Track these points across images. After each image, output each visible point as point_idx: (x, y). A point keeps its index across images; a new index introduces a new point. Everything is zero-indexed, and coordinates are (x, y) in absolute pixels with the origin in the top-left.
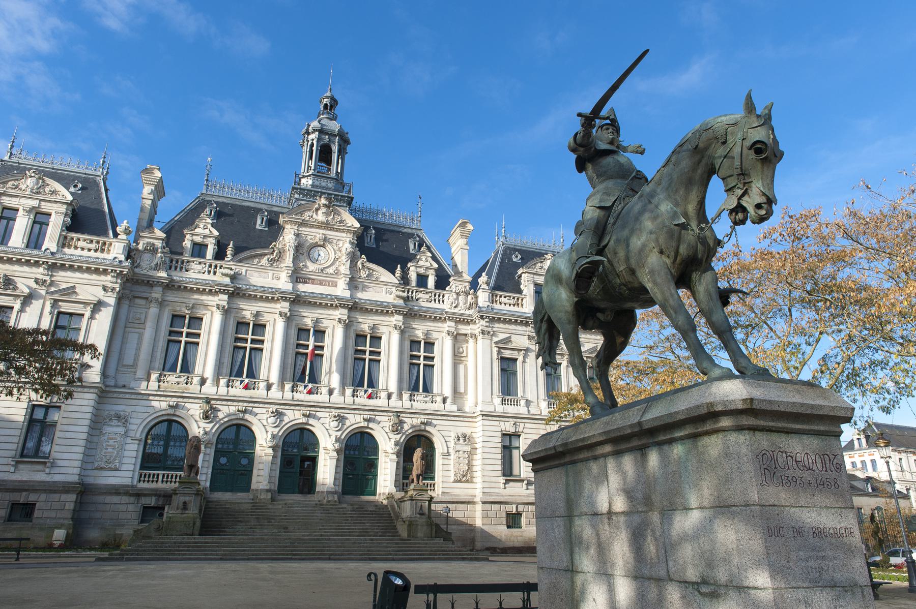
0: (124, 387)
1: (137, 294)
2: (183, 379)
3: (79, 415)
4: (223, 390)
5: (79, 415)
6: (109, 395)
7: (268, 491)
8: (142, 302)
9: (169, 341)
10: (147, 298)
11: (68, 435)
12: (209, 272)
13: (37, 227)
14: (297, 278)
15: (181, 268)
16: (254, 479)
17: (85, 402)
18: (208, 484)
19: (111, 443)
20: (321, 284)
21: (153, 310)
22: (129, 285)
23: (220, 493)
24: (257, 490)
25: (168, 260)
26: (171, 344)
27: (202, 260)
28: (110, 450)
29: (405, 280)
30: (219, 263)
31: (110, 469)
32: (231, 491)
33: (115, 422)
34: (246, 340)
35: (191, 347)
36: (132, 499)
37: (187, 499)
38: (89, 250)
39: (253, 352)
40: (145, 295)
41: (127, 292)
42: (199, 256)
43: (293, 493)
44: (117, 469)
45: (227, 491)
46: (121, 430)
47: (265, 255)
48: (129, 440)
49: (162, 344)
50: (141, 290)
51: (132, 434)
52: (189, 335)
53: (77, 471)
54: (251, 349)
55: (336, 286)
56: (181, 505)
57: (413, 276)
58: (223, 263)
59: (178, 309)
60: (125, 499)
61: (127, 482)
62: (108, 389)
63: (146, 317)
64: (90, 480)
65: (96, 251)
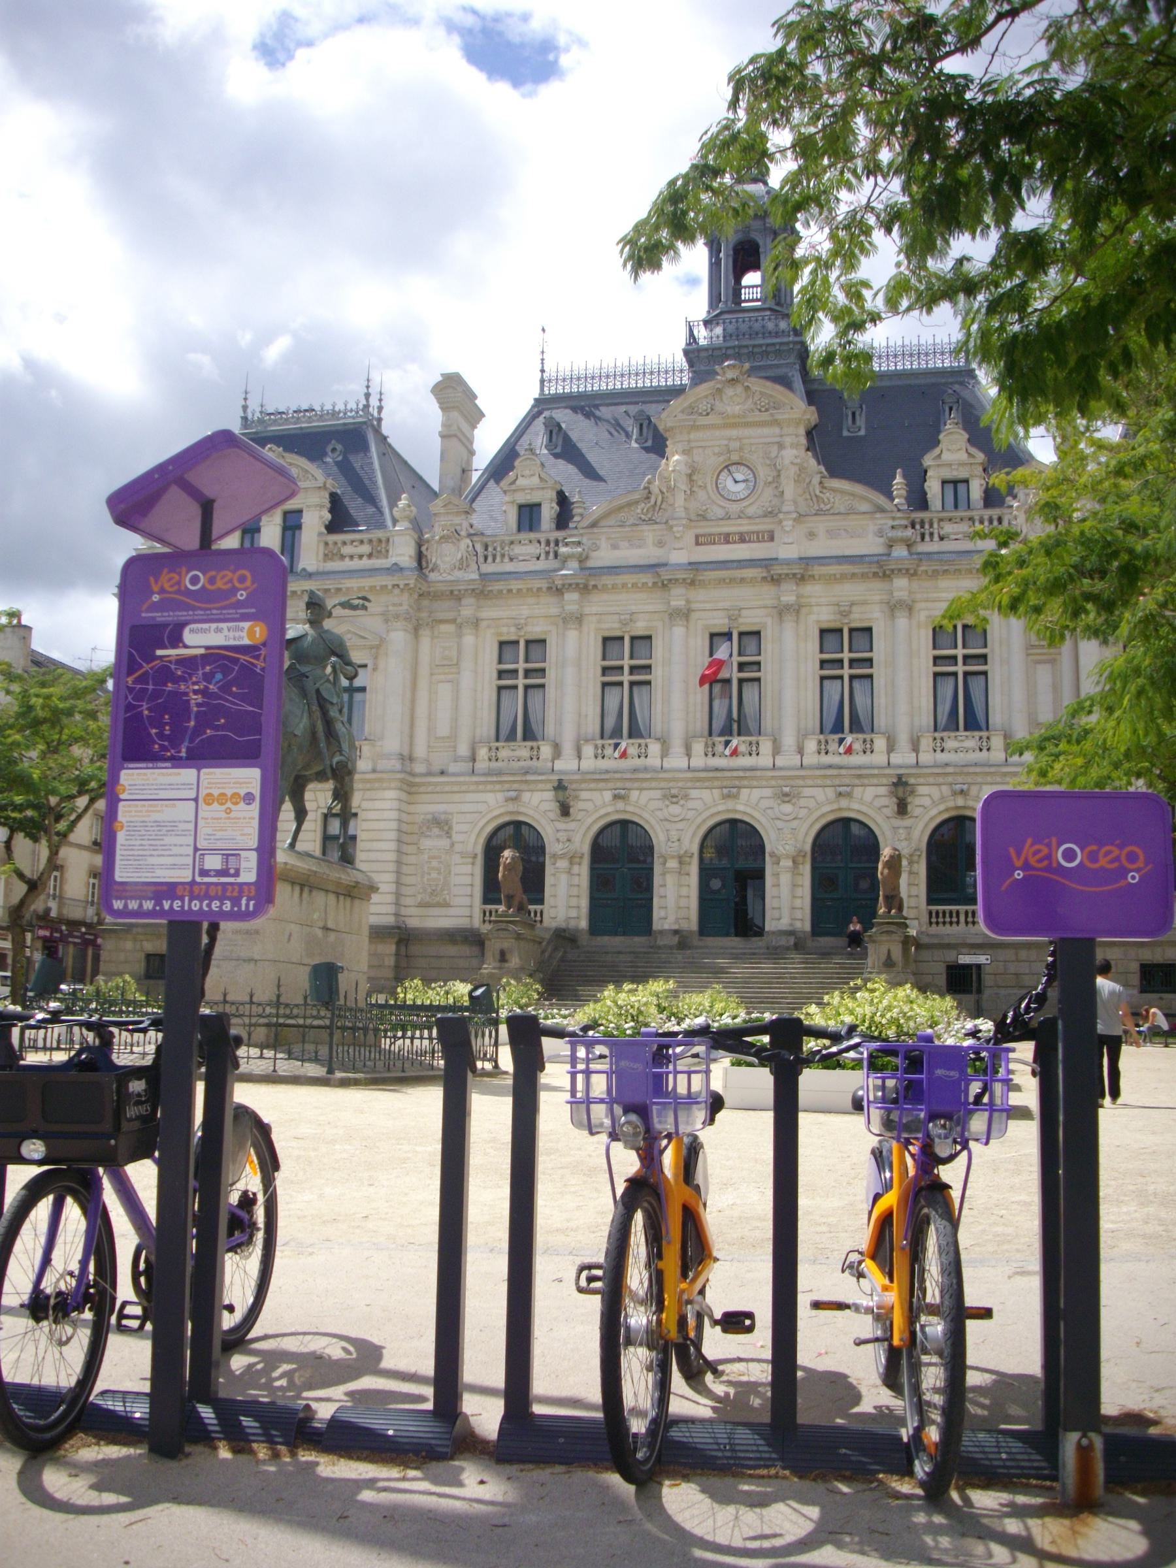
0: (442, 773)
1: (441, 616)
2: (525, 753)
3: (382, 825)
4: (588, 763)
5: (382, 825)
6: (422, 789)
7: (676, 932)
8: (450, 628)
9: (500, 688)
10: (453, 621)
11: (372, 856)
12: (547, 553)
13: (289, 533)
14: (697, 537)
15: (503, 556)
16: (657, 914)
17: (387, 805)
18: (584, 924)
19: (435, 863)
20: (742, 540)
21: (469, 640)
22: (425, 603)
23: (606, 938)
24: (661, 932)
25: (479, 547)
26: (504, 693)
27: (532, 535)
28: (434, 875)
29: (919, 500)
30: (560, 535)
31: (438, 905)
32: (624, 934)
33: (436, 831)
34: (621, 668)
35: (535, 695)
36: (475, 950)
37: (506, 945)
38: (361, 557)
39: (635, 689)
40: (450, 615)
41: (424, 615)
42: (531, 530)
43: (727, 935)
44: (447, 905)
45: (616, 934)
46: (444, 843)
47: (637, 502)
48: (456, 858)
49: (489, 695)
50: (443, 609)
51: (458, 848)
52: (528, 673)
53: (391, 909)
54: (632, 684)
55: (772, 539)
56: (498, 957)
57: (933, 487)
58: (568, 532)
59: (505, 630)
60: (466, 950)
61: (463, 923)
62: (417, 780)
63: (459, 652)
64: (413, 923)
65: (370, 556)
